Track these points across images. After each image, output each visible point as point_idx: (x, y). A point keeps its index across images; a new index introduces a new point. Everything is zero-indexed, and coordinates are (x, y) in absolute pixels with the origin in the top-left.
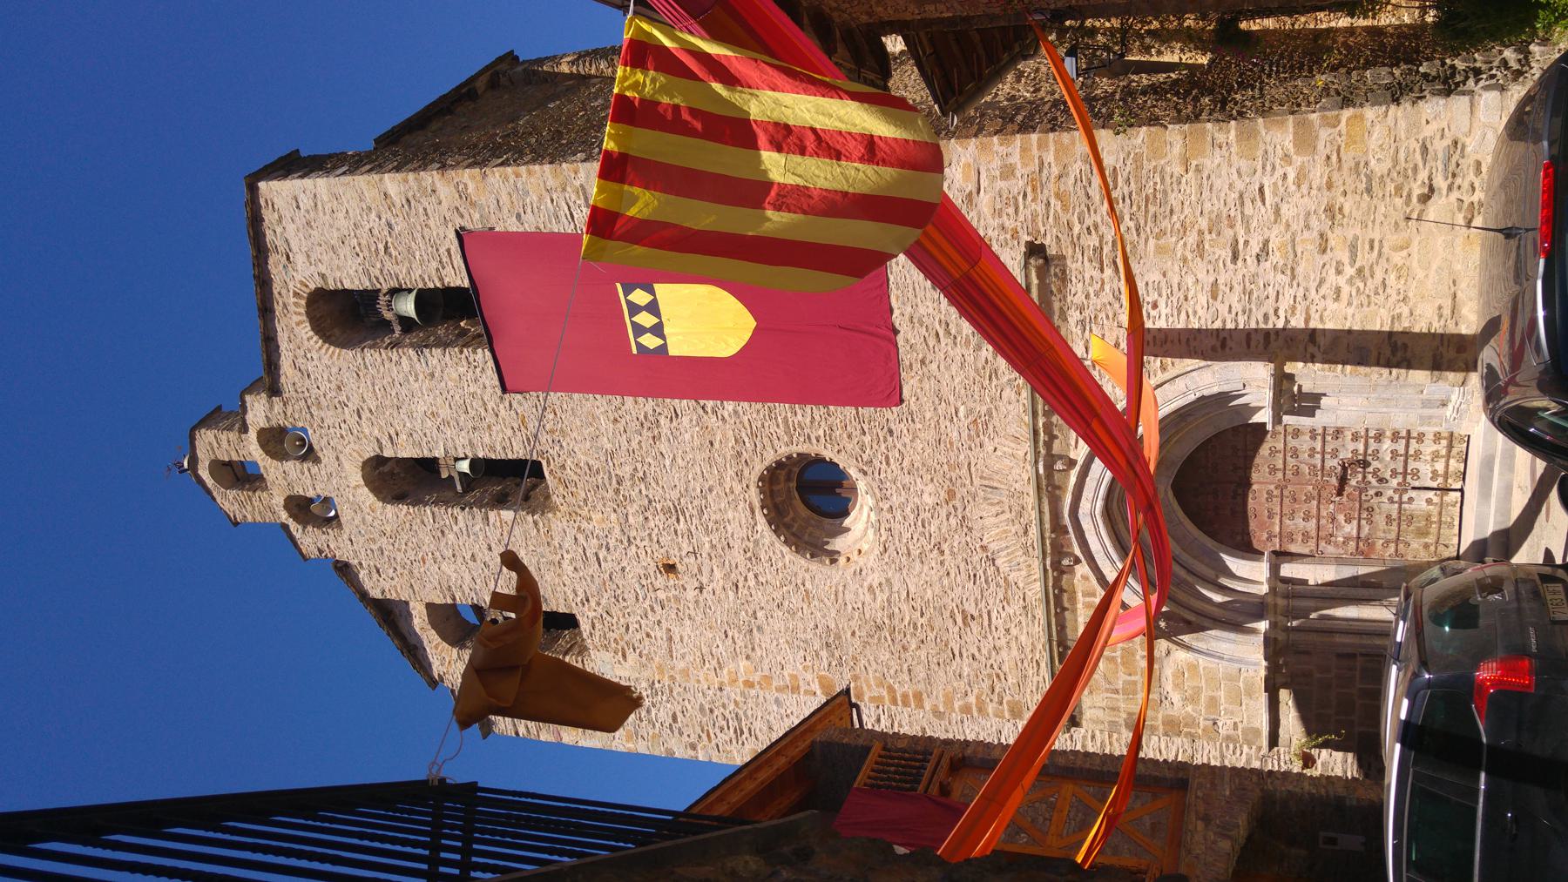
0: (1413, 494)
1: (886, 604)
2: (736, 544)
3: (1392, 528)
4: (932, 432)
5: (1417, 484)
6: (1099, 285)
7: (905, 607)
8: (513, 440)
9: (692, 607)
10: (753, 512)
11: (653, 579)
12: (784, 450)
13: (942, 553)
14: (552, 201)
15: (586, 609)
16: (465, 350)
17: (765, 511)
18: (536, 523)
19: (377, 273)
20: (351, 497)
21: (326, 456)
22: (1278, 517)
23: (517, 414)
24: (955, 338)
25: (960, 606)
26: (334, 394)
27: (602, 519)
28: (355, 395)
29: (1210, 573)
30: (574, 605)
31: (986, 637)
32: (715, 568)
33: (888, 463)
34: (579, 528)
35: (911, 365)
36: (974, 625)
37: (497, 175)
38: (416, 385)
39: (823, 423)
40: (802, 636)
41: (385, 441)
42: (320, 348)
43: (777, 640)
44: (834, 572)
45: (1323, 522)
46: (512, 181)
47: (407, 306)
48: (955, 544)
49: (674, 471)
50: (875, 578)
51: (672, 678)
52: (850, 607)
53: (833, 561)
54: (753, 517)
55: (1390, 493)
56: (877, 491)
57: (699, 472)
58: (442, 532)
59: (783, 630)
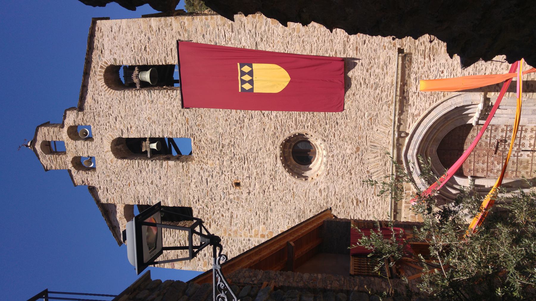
0: (522, 153)
1: (326, 197)
2: (267, 173)
4: (354, 123)
5: (523, 149)
6: (423, 65)
7: (333, 198)
8: (181, 129)
9: (244, 201)
10: (276, 159)
11: (229, 189)
12: (293, 132)
13: (351, 174)
14: (218, 30)
15: (197, 205)
16: (169, 91)
17: (281, 158)
18: (183, 166)
19: (139, 58)
20: (103, 156)
21: (97, 138)
22: (473, 163)
23: (185, 118)
24: (367, 85)
26: (107, 110)
27: (212, 163)
28: (117, 111)
30: (192, 203)
31: (365, 210)
32: (257, 183)
33: (334, 137)
34: (202, 168)
35: (349, 96)
36: (360, 205)
37: (198, 19)
38: (145, 106)
39: (311, 120)
40: (289, 213)
41: (125, 131)
42: (106, 90)
43: (278, 215)
44: (306, 183)
45: (489, 164)
46: (204, 21)
47: (146, 76)
48: (357, 170)
49: (247, 141)
50: (322, 186)
51: (230, 235)
52: (310, 199)
53: (306, 179)
54: (276, 161)
55: (514, 152)
56: (328, 148)
57: (257, 142)
58: (141, 171)
59: (281, 210)
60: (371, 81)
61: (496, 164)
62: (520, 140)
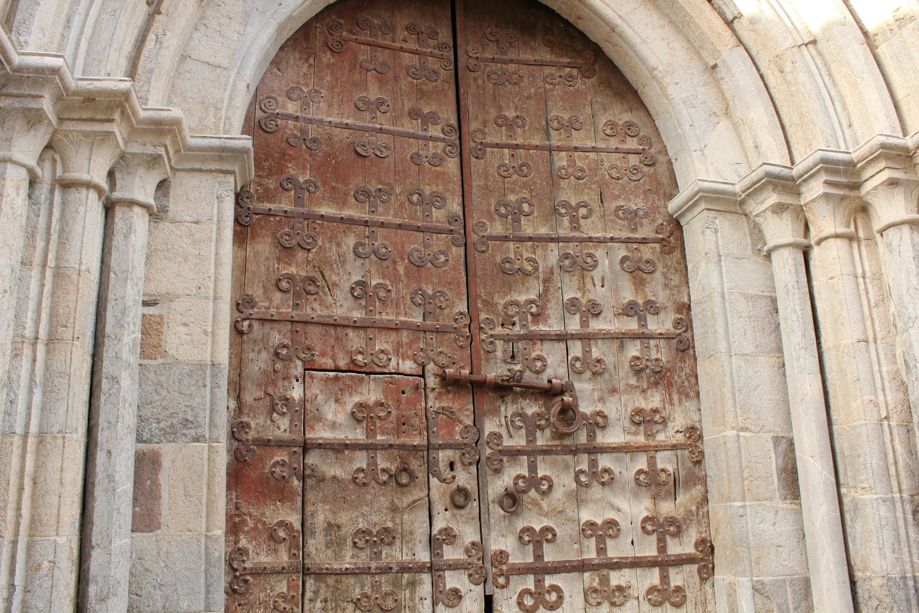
3: (348, 553)
22: (367, 217)
45: (355, 340)
61: (357, 399)
62: (581, 567)
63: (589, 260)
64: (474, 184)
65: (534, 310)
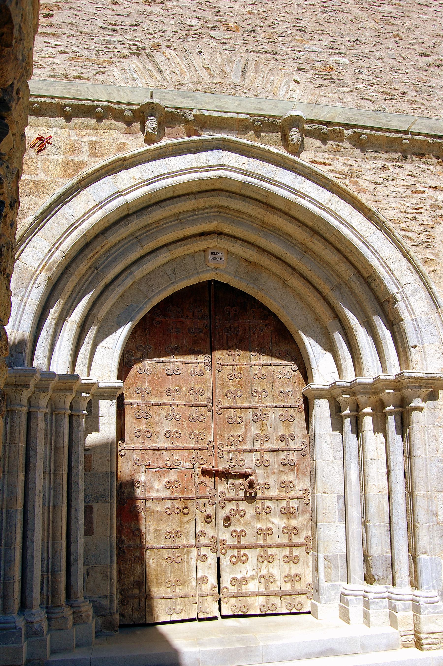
3: (163, 540)
5: (225, 562)
22: (171, 402)
24: (425, 70)
25: (67, 6)
29: (102, 313)
60: (438, 81)
61: (167, 479)
63: (265, 416)
64: (217, 383)
65: (240, 439)
